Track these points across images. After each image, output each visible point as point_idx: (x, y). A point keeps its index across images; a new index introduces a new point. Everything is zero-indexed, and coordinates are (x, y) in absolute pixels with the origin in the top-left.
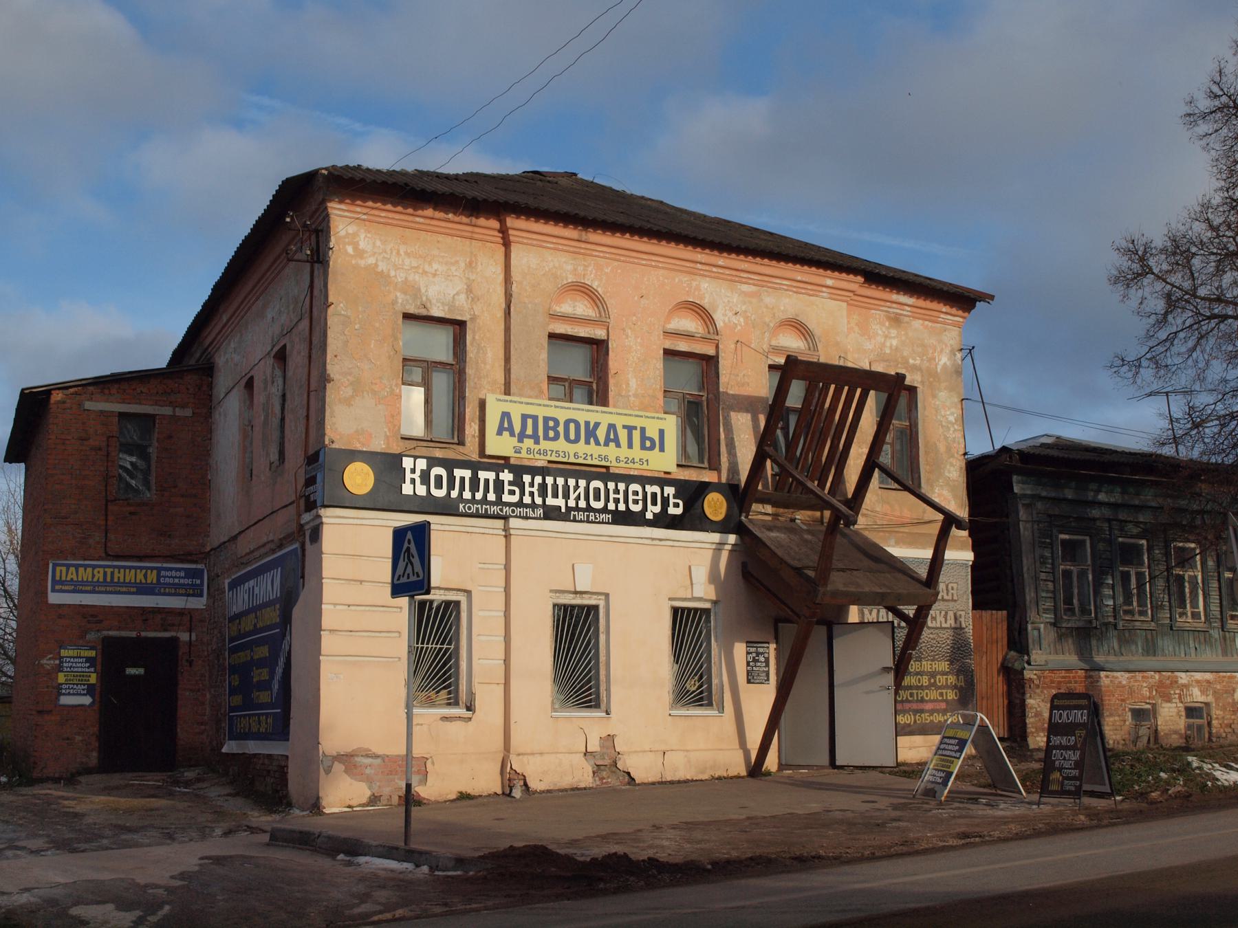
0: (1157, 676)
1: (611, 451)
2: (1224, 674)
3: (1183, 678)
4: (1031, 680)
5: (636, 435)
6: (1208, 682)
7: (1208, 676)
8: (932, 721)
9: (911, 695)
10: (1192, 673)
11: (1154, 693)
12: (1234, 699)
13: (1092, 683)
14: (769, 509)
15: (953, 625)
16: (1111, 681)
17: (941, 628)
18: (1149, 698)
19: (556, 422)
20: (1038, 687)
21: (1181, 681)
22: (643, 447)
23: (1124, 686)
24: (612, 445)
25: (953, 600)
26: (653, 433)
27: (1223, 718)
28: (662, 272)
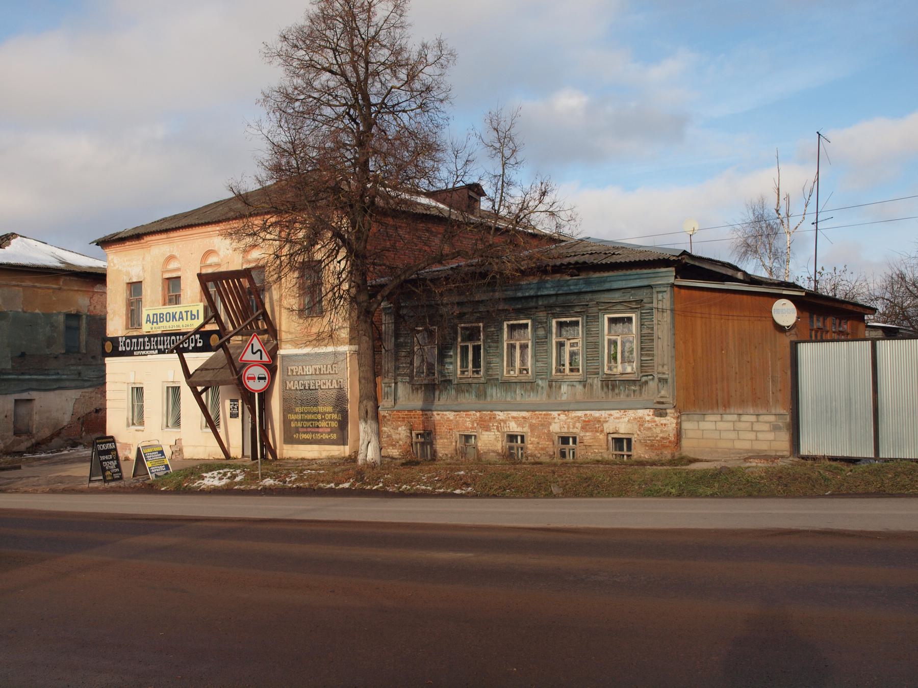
0: (478, 414)
1: (181, 323)
2: (541, 412)
3: (501, 415)
4: (385, 417)
5: (189, 314)
6: (524, 418)
7: (524, 414)
8: (322, 438)
9: (312, 424)
10: (510, 412)
11: (475, 425)
12: (549, 431)
13: (426, 418)
14: (240, 338)
15: (336, 387)
16: (441, 417)
17: (329, 389)
18: (471, 428)
19: (163, 314)
20: (389, 420)
21: (498, 417)
22: (191, 319)
23: (451, 421)
24: (181, 320)
25: (335, 374)
26: (195, 313)
27: (538, 443)
28: (200, 240)
